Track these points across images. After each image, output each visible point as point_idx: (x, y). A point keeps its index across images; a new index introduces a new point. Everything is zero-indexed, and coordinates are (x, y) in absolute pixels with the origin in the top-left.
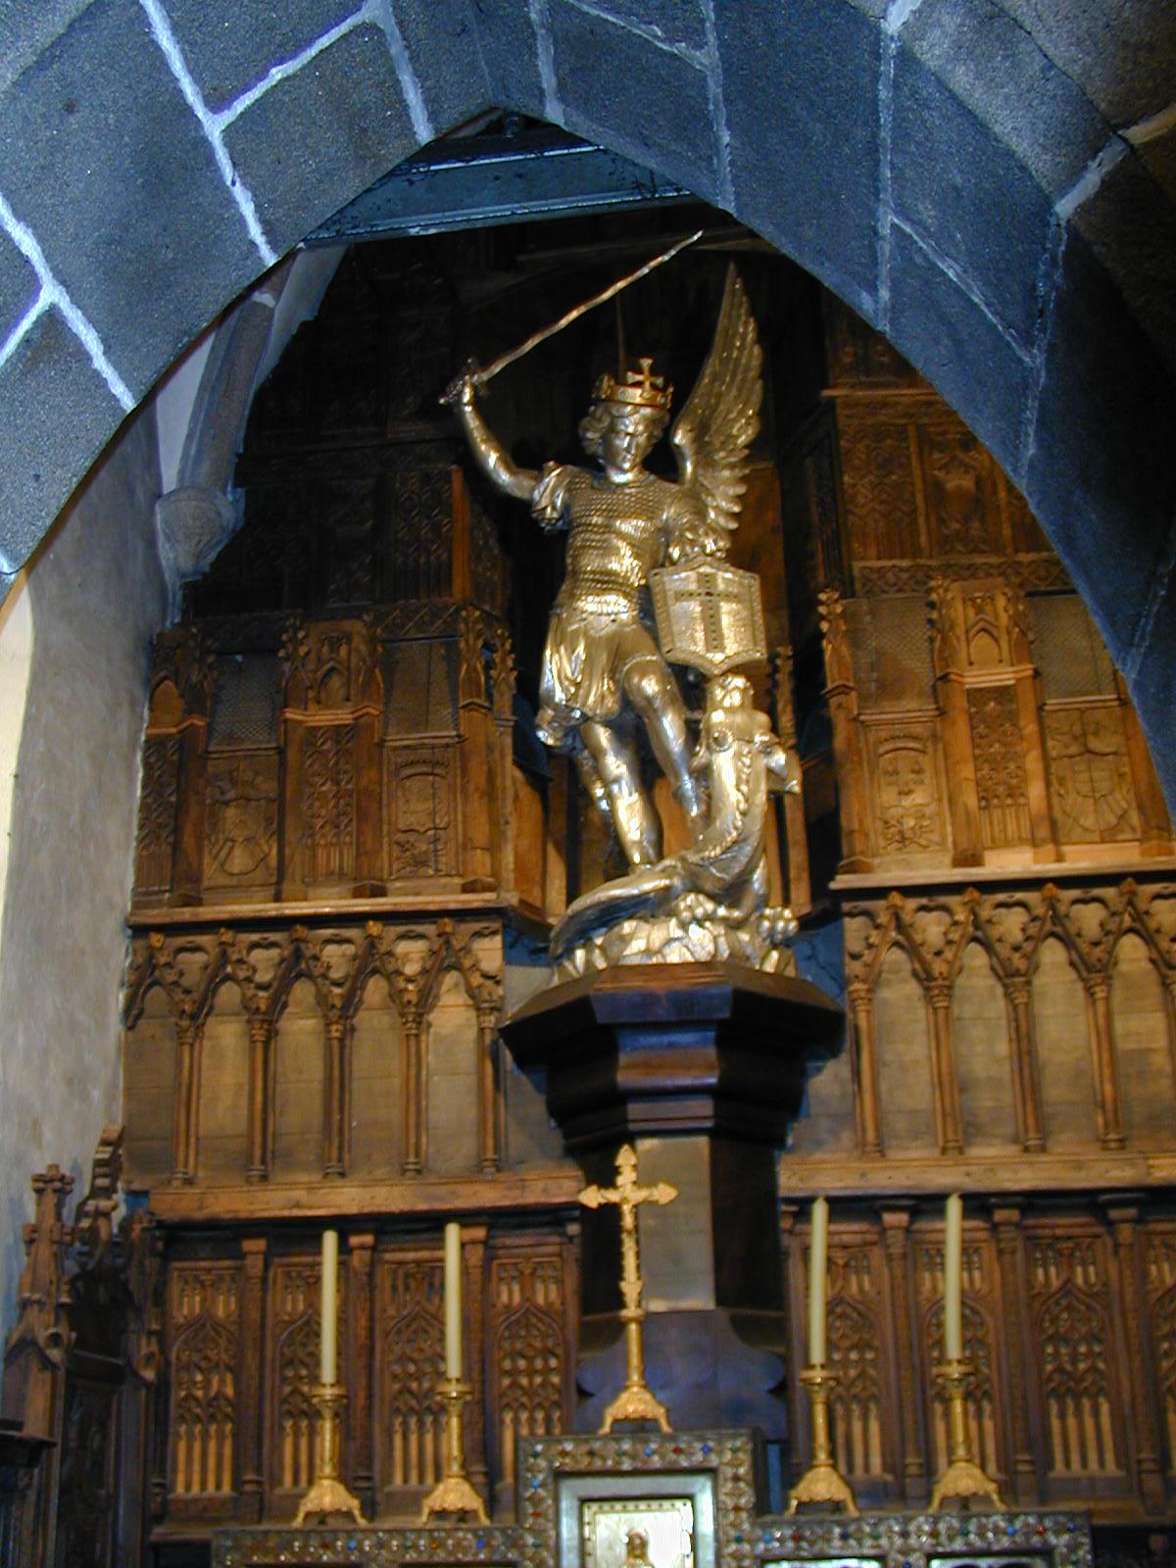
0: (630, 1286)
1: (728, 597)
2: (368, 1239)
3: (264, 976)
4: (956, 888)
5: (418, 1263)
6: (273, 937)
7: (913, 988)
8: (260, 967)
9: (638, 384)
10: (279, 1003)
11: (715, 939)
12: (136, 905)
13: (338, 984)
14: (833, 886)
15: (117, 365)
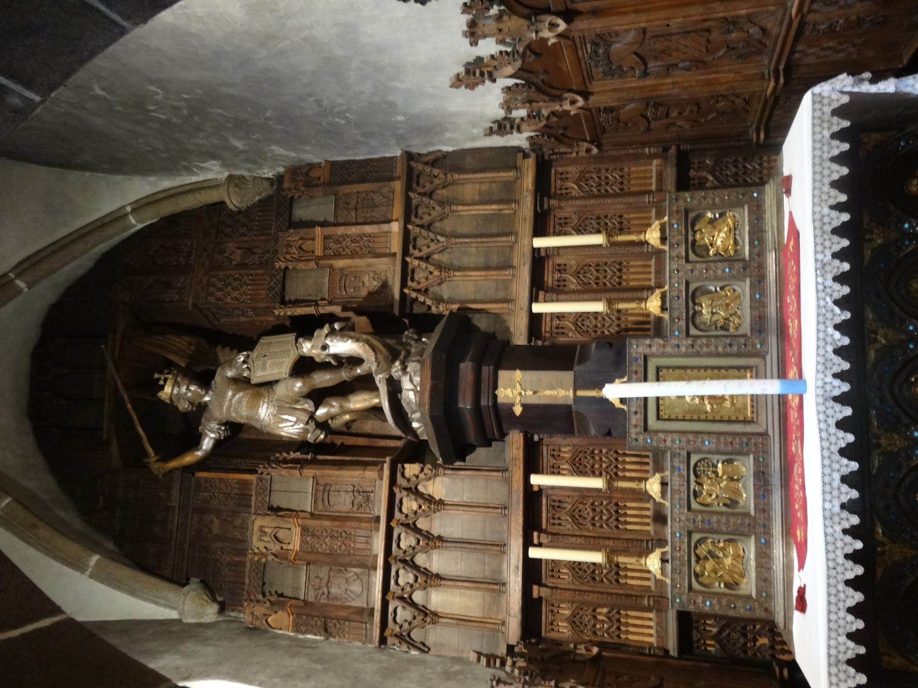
2: (535, 534)
3: (411, 579)
5: (548, 511)
6: (393, 573)
13: (418, 541)
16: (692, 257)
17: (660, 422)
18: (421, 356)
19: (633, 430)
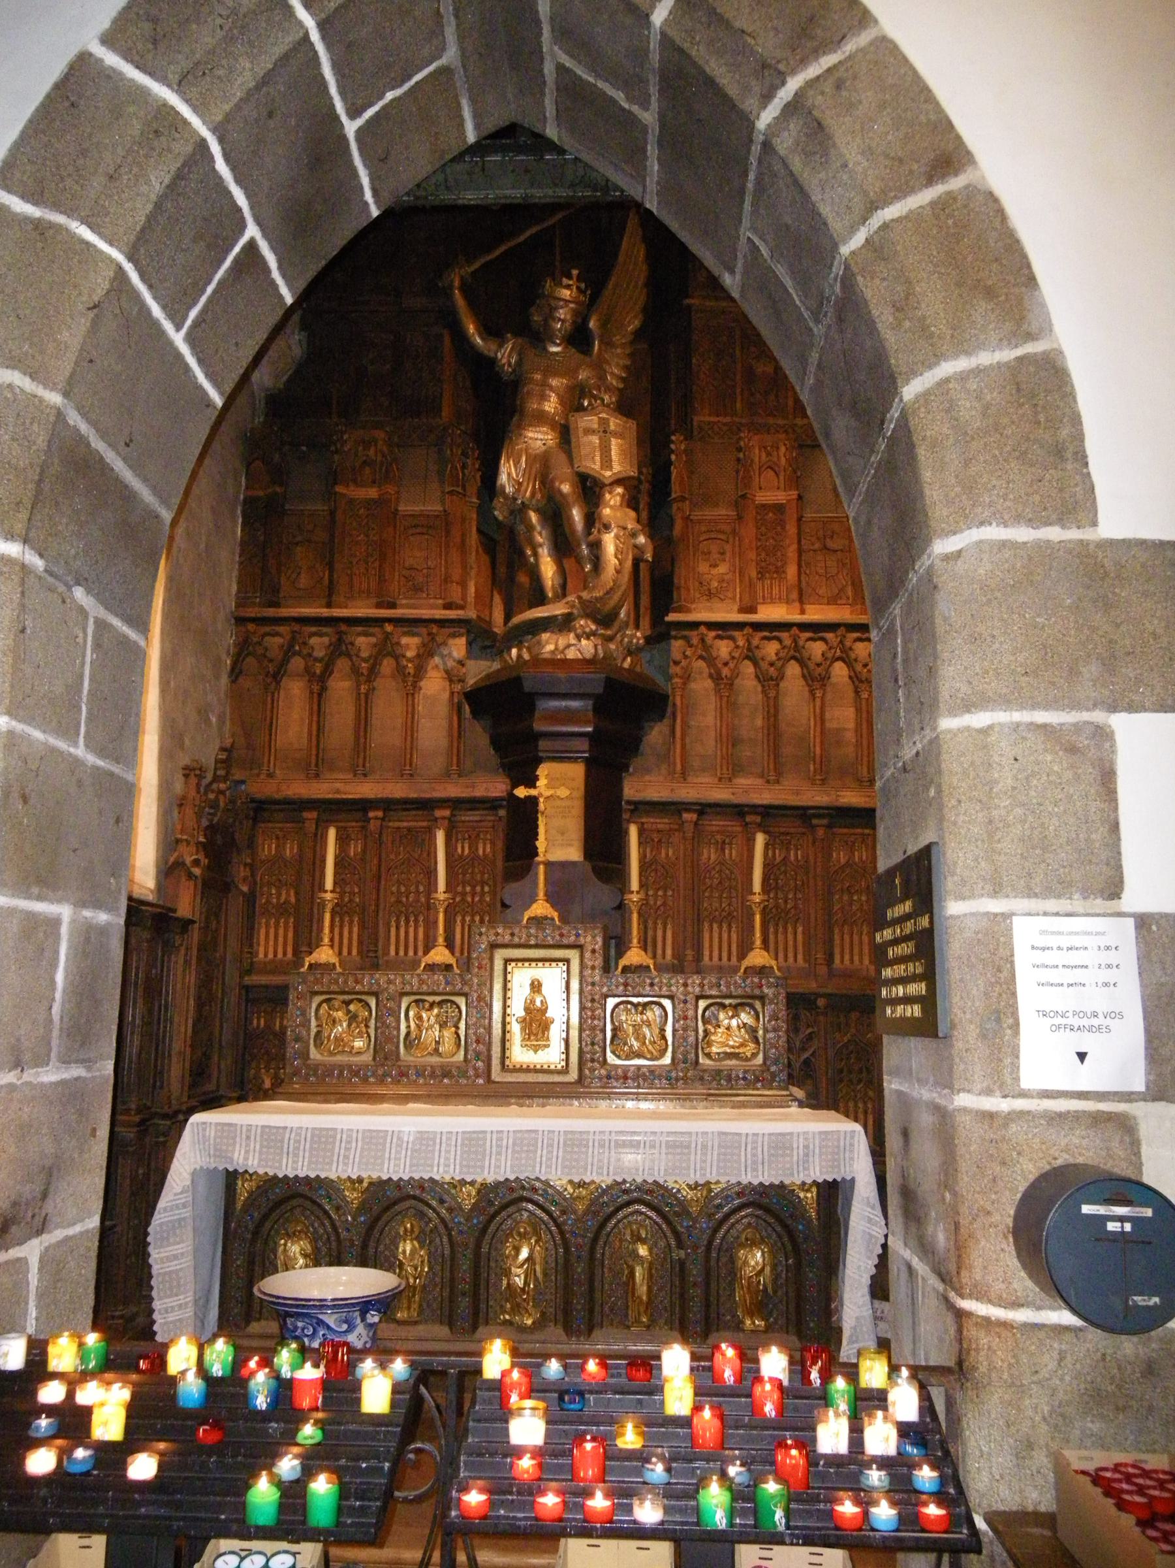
0: (541, 844)
1: (616, 434)
2: (380, 814)
3: (319, 653)
4: (739, 626)
5: (409, 829)
6: (325, 630)
7: (709, 684)
8: (316, 647)
9: (568, 287)
10: (328, 670)
11: (596, 646)
12: (238, 606)
14: (667, 619)
15: (284, 276)
16: (702, 1004)
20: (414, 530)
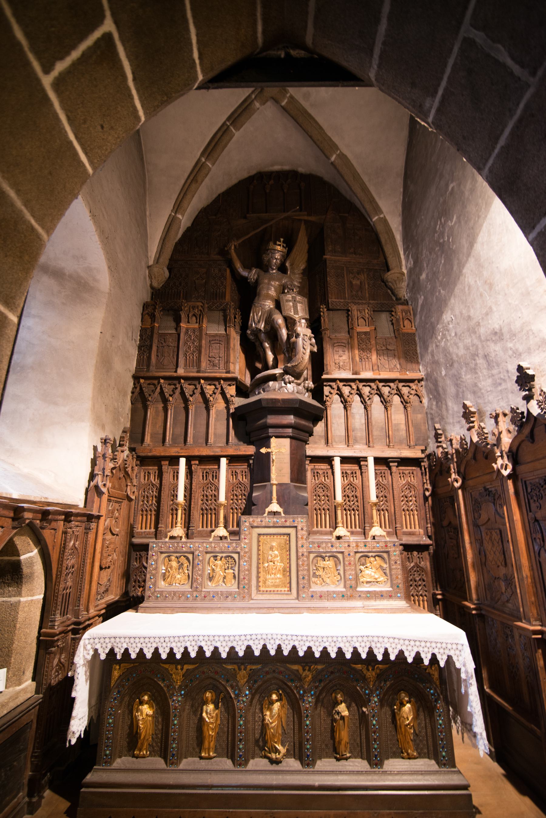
1: (299, 302)
4: (353, 380)
9: (280, 245)
14: (322, 377)
16: (359, 555)
17: (257, 535)
18: (297, 392)
19: (251, 520)
20: (213, 342)
